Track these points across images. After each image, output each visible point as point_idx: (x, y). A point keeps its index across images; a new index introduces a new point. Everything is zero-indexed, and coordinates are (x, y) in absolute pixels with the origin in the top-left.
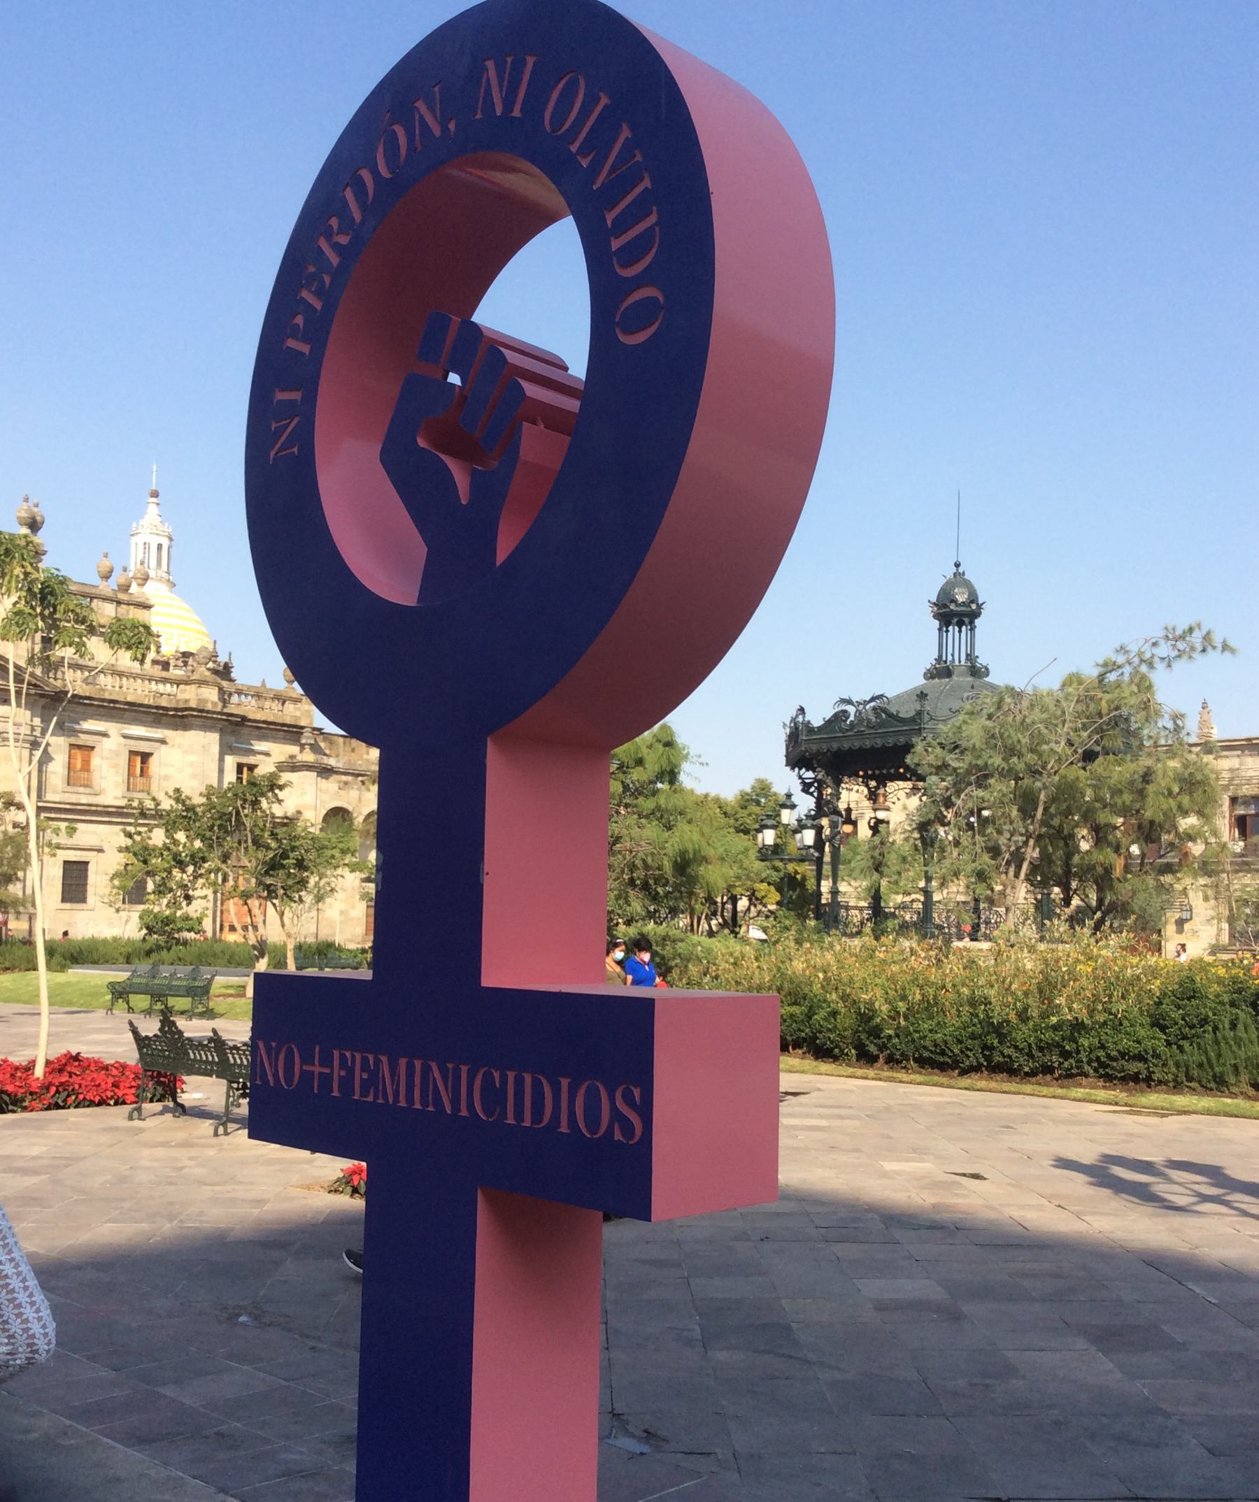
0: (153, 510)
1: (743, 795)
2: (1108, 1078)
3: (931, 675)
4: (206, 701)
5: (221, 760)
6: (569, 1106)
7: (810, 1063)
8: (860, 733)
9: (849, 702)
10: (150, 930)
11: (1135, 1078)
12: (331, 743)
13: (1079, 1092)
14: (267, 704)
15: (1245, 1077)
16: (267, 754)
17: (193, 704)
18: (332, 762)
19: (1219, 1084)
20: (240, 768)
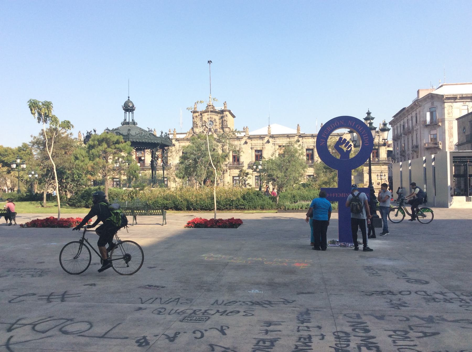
1: (19, 148)
2: (237, 209)
9: (109, 130)
11: (242, 209)
13: (234, 212)
19: (255, 208)
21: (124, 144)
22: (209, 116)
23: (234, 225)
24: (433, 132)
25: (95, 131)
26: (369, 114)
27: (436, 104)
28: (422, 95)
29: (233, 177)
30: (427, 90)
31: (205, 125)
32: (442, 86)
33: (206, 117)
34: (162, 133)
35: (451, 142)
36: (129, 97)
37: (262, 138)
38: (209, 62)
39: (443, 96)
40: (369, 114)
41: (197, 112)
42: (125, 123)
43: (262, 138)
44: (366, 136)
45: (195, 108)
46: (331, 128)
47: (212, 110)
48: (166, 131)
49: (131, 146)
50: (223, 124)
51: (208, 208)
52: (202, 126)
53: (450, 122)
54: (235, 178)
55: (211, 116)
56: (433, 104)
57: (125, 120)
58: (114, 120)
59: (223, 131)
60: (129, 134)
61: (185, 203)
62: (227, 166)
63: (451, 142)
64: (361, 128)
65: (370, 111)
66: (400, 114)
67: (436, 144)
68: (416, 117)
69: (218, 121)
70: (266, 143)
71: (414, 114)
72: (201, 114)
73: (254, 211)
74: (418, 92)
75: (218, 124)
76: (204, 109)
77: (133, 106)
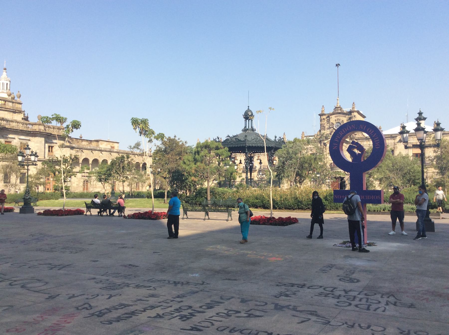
0: (4, 74)
4: (41, 129)
5: (45, 145)
6: (373, 197)
7: (263, 210)
8: (232, 144)
9: (229, 137)
10: (56, 190)
12: (72, 140)
14: (56, 130)
15: (341, 208)
16: (56, 143)
17: (37, 130)
18: (74, 145)
20: (49, 147)
21: (223, 150)
23: (285, 223)
25: (218, 138)
26: (420, 114)
31: (333, 127)
33: (333, 119)
34: (276, 137)
36: (248, 107)
37: (393, 137)
38: (337, 65)
40: (420, 114)
41: (325, 115)
42: (245, 130)
43: (393, 137)
44: (377, 139)
45: (322, 111)
46: (343, 132)
47: (340, 111)
48: (280, 135)
49: (229, 151)
51: (265, 207)
52: (330, 128)
55: (339, 118)
58: (234, 128)
60: (245, 140)
64: (372, 131)
65: (422, 111)
70: (398, 142)
72: (328, 117)
73: (336, 212)
76: (331, 111)
77: (252, 115)
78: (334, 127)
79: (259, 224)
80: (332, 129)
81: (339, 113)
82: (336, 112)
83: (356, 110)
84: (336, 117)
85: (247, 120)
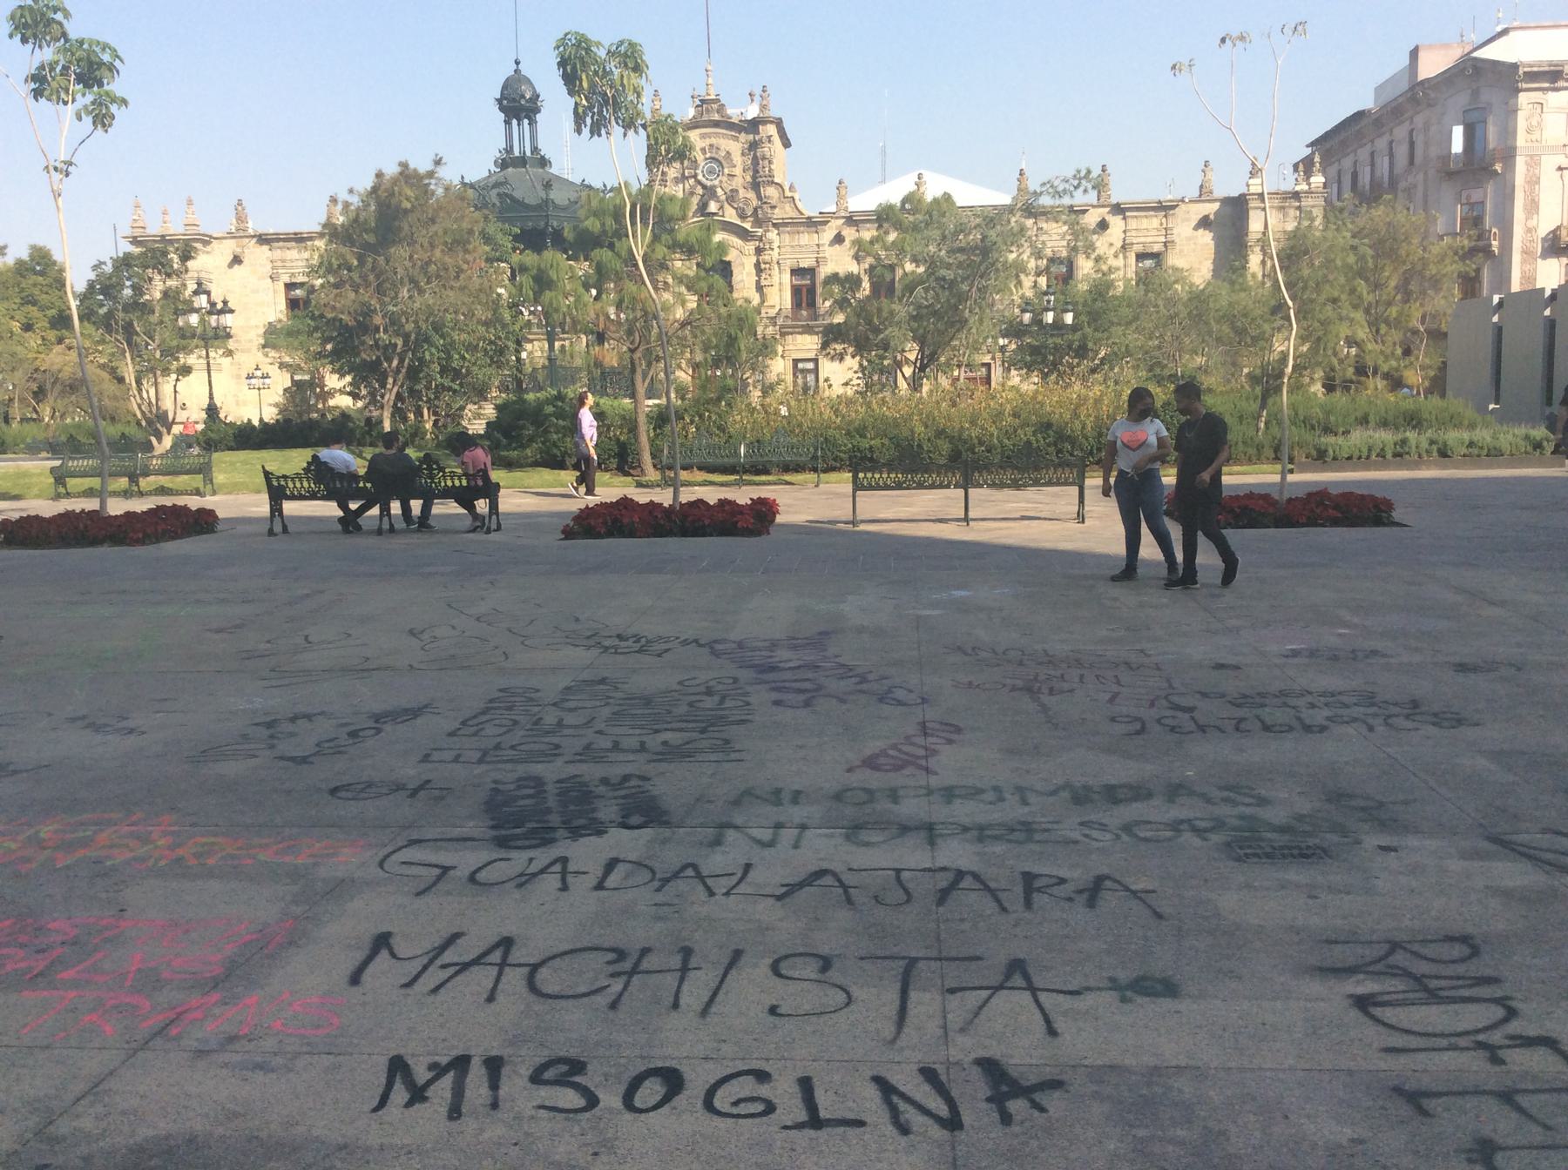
3: (504, 164)
22: (708, 141)
24: (1476, 195)
27: (1487, 96)
28: (1432, 66)
29: (796, 361)
30: (1446, 46)
31: (695, 176)
32: (1505, 32)
35: (1529, 230)
36: (517, 63)
39: (1514, 67)
42: (508, 161)
47: (716, 117)
50: (756, 171)
52: (683, 178)
53: (1534, 161)
54: (800, 366)
55: (713, 141)
56: (1476, 94)
57: (509, 150)
59: (759, 197)
61: (945, 447)
62: (775, 324)
63: (1529, 230)
66: (1343, 135)
67: (1483, 236)
68: (1412, 144)
69: (737, 159)
71: (1401, 132)
74: (1414, 54)
75: (738, 171)
78: (700, 177)
79: (1312, 522)
80: (692, 181)
81: (716, 124)
82: (705, 118)
83: (774, 112)
84: (703, 136)
85: (515, 122)
